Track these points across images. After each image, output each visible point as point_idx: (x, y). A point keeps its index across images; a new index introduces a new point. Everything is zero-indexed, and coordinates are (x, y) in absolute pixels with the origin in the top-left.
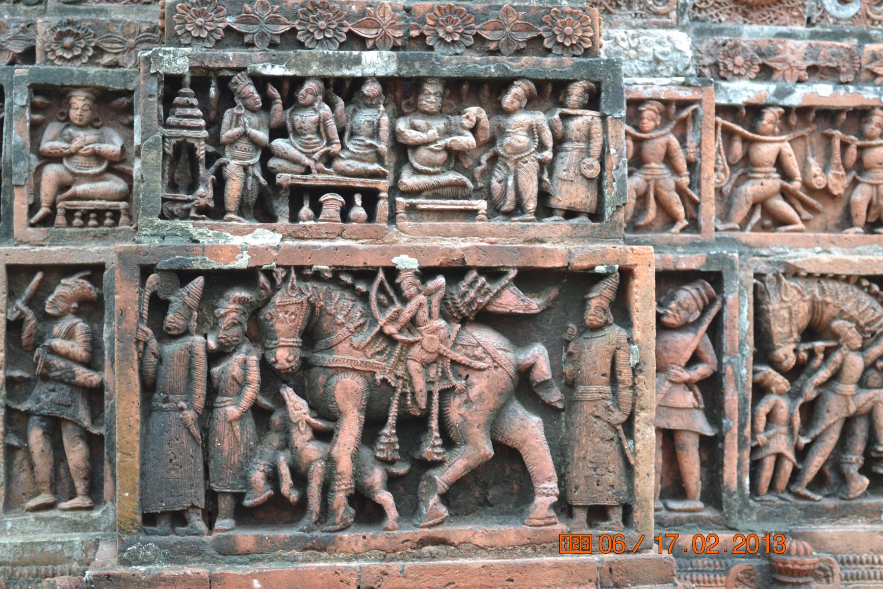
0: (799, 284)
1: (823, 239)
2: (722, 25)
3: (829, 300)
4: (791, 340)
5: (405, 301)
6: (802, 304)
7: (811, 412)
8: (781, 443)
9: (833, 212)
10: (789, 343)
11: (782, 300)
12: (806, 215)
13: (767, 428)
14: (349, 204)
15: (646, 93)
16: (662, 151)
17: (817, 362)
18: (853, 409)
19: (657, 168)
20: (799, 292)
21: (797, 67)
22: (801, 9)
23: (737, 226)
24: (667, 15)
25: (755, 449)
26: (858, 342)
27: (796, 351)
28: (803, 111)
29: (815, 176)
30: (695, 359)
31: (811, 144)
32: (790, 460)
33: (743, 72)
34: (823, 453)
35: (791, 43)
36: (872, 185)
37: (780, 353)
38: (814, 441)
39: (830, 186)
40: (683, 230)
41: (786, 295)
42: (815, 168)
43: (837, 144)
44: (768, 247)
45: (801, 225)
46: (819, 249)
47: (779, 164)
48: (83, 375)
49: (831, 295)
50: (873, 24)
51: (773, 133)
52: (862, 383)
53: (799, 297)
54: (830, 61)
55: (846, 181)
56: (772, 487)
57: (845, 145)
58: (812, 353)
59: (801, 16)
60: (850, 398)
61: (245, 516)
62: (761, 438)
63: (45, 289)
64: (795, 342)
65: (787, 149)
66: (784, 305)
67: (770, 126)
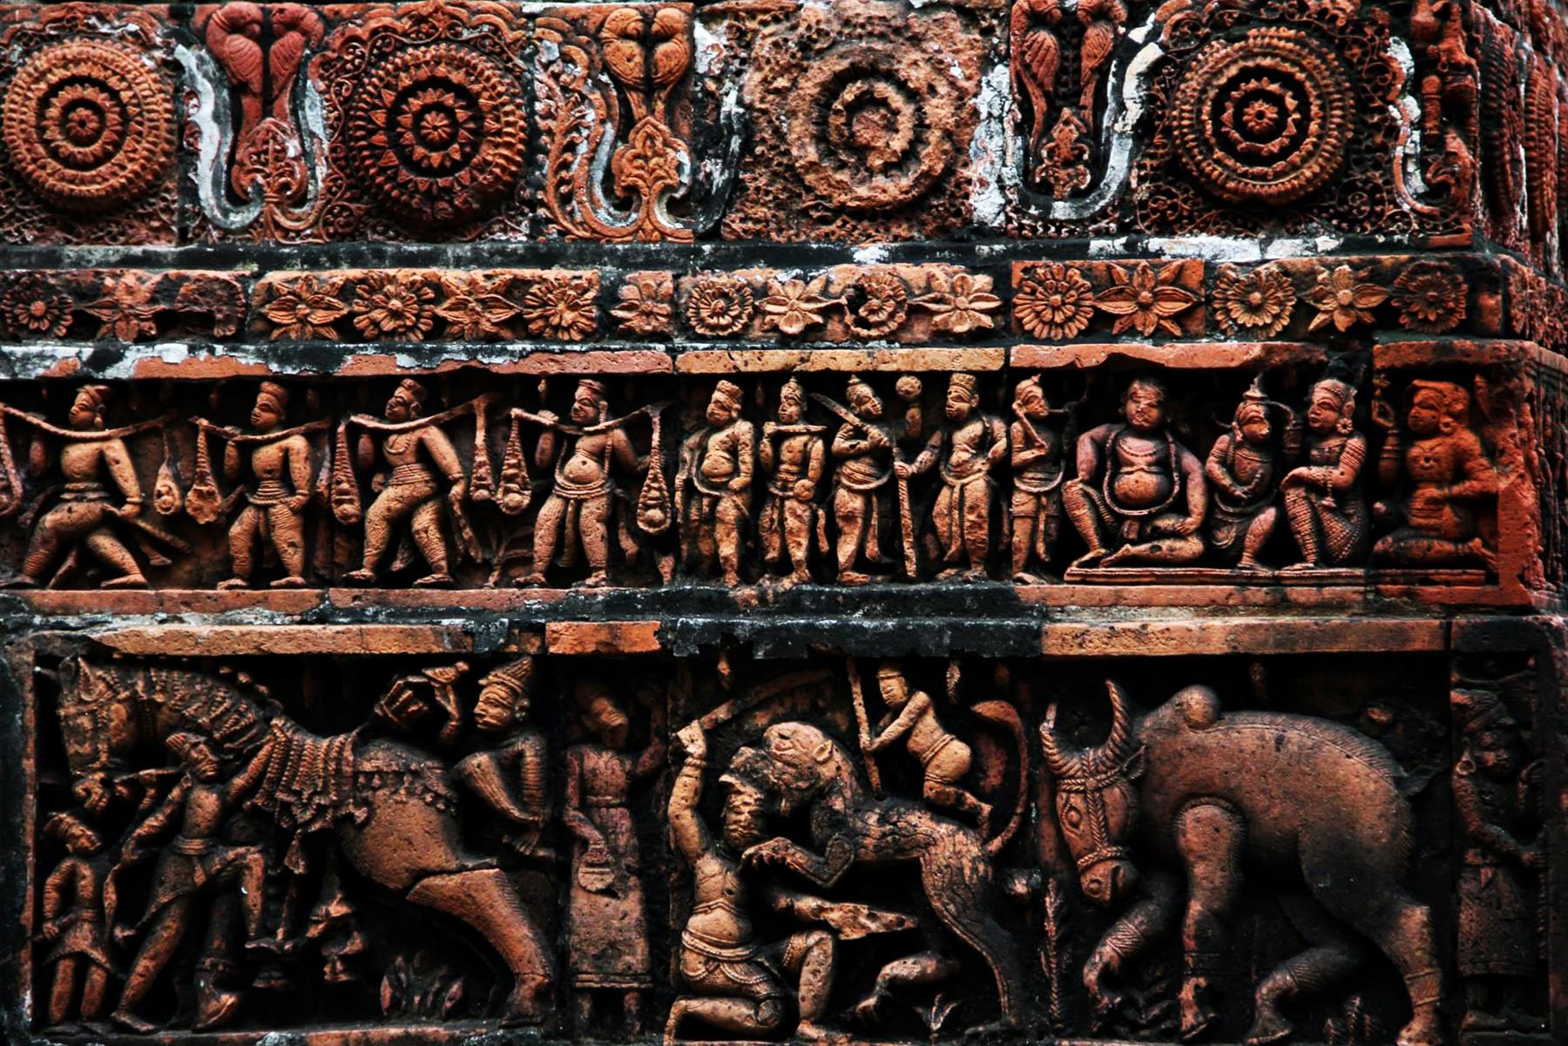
0: (112, 675)
1: (171, 598)
2: (26, 248)
3: (159, 698)
4: (97, 765)
6: (115, 706)
10: (95, 771)
11: (81, 702)
12: (158, 560)
20: (109, 687)
21: (136, 316)
22: (164, 217)
23: (28, 580)
27: (107, 783)
29: (160, 495)
31: (171, 440)
32: (99, 966)
33: (45, 325)
34: (152, 953)
35: (130, 277)
36: (258, 507)
39: (189, 510)
41: (88, 692)
42: (164, 481)
43: (201, 438)
44: (78, 614)
45: (137, 577)
46: (163, 616)
49: (163, 691)
50: (285, 237)
52: (220, 833)
53: (109, 694)
54: (196, 302)
56: (72, 1014)
57: (216, 444)
58: (138, 787)
59: (165, 228)
60: (195, 860)
62: (50, 927)
64: (102, 768)
65: (116, 450)
66: (83, 708)
67: (84, 414)
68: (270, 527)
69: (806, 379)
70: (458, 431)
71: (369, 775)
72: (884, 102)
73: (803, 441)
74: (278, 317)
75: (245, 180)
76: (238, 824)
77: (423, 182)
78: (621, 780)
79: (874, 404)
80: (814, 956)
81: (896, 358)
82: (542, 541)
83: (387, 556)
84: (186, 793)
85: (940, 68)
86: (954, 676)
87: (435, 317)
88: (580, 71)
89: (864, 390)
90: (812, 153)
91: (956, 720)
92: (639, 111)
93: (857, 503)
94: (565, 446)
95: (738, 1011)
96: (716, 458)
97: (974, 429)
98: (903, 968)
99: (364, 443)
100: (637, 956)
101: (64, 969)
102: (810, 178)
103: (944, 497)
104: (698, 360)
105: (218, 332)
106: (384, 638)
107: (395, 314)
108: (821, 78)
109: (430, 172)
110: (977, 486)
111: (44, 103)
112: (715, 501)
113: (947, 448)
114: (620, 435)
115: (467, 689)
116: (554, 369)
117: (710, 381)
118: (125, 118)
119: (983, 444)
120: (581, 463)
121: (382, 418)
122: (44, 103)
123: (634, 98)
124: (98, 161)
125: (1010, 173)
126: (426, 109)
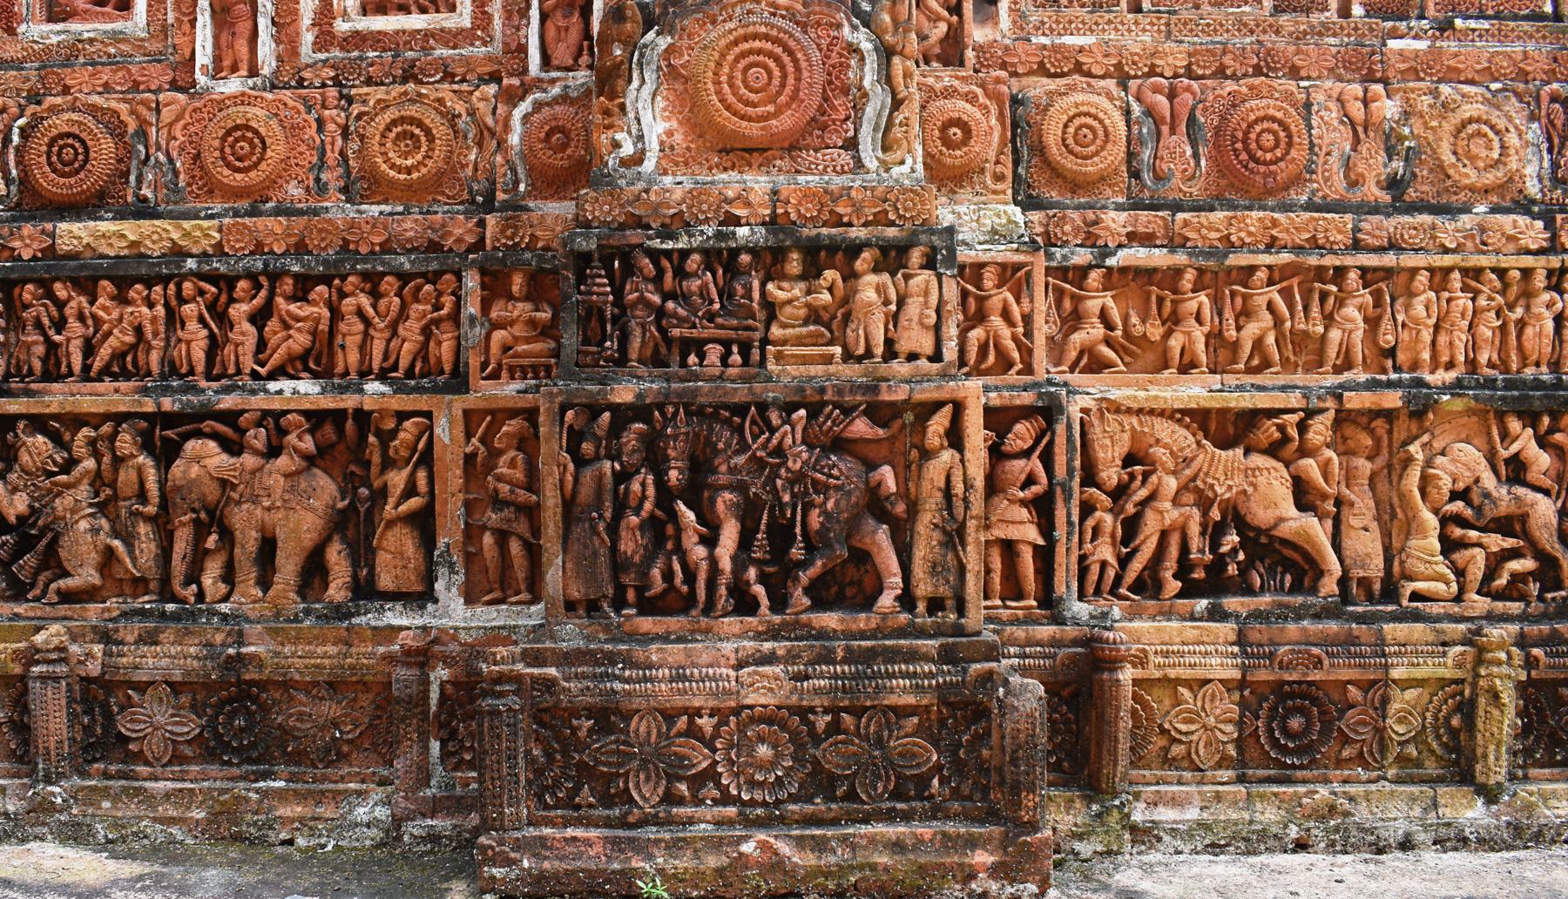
5: (773, 431)
7: (1131, 527)
8: (1105, 552)
9: (1150, 357)
12: (1127, 359)
13: (1092, 541)
14: (728, 353)
15: (986, 257)
16: (1000, 306)
17: (1138, 483)
18: (1168, 522)
19: (997, 321)
24: (1004, 192)
25: (1082, 558)
26: (1171, 465)
28: (1124, 270)
30: (1030, 480)
37: (1104, 475)
38: (1135, 551)
40: (1018, 373)
42: (1134, 320)
43: (1154, 298)
47: (1104, 316)
48: (522, 495)
51: (1097, 290)
55: (1161, 330)
56: (1098, 592)
57: (1160, 300)
61: (648, 607)
63: (493, 429)
65: (1110, 303)
68: (1191, 342)
69: (1465, 272)
70: (1287, 294)
71: (1253, 470)
72: (1485, 135)
73: (1463, 301)
74: (1191, 235)
75: (1165, 167)
76: (1189, 498)
77: (1262, 169)
78: (1368, 473)
79: (1498, 284)
80: (1477, 562)
81: (1505, 262)
82: (1332, 352)
83: (1251, 357)
84: (1159, 478)
85: (1510, 119)
86: (1546, 420)
87: (1272, 236)
88: (1334, 115)
89: (1494, 276)
90: (1453, 159)
91: (1542, 442)
92: (1362, 136)
93: (1489, 333)
94: (1340, 303)
95: (1441, 587)
96: (1419, 309)
97: (1546, 297)
98: (1515, 565)
99: (1239, 301)
100: (1378, 562)
101: (1095, 569)
102: (1451, 172)
103: (1529, 331)
104: (1410, 260)
105: (1158, 242)
106: (1262, 401)
107: (1250, 234)
108: (1453, 122)
109: (1266, 163)
110: (1549, 325)
111: (1066, 126)
112: (1419, 332)
113: (1528, 308)
114: (1369, 299)
115: (1302, 427)
116: (1338, 263)
117: (1414, 271)
118: (1107, 134)
119: (1549, 306)
120: (1351, 311)
121: (1246, 287)
122: (1066, 126)
123: (1360, 129)
124: (1091, 157)
125: (1546, 172)
126: (1263, 131)
